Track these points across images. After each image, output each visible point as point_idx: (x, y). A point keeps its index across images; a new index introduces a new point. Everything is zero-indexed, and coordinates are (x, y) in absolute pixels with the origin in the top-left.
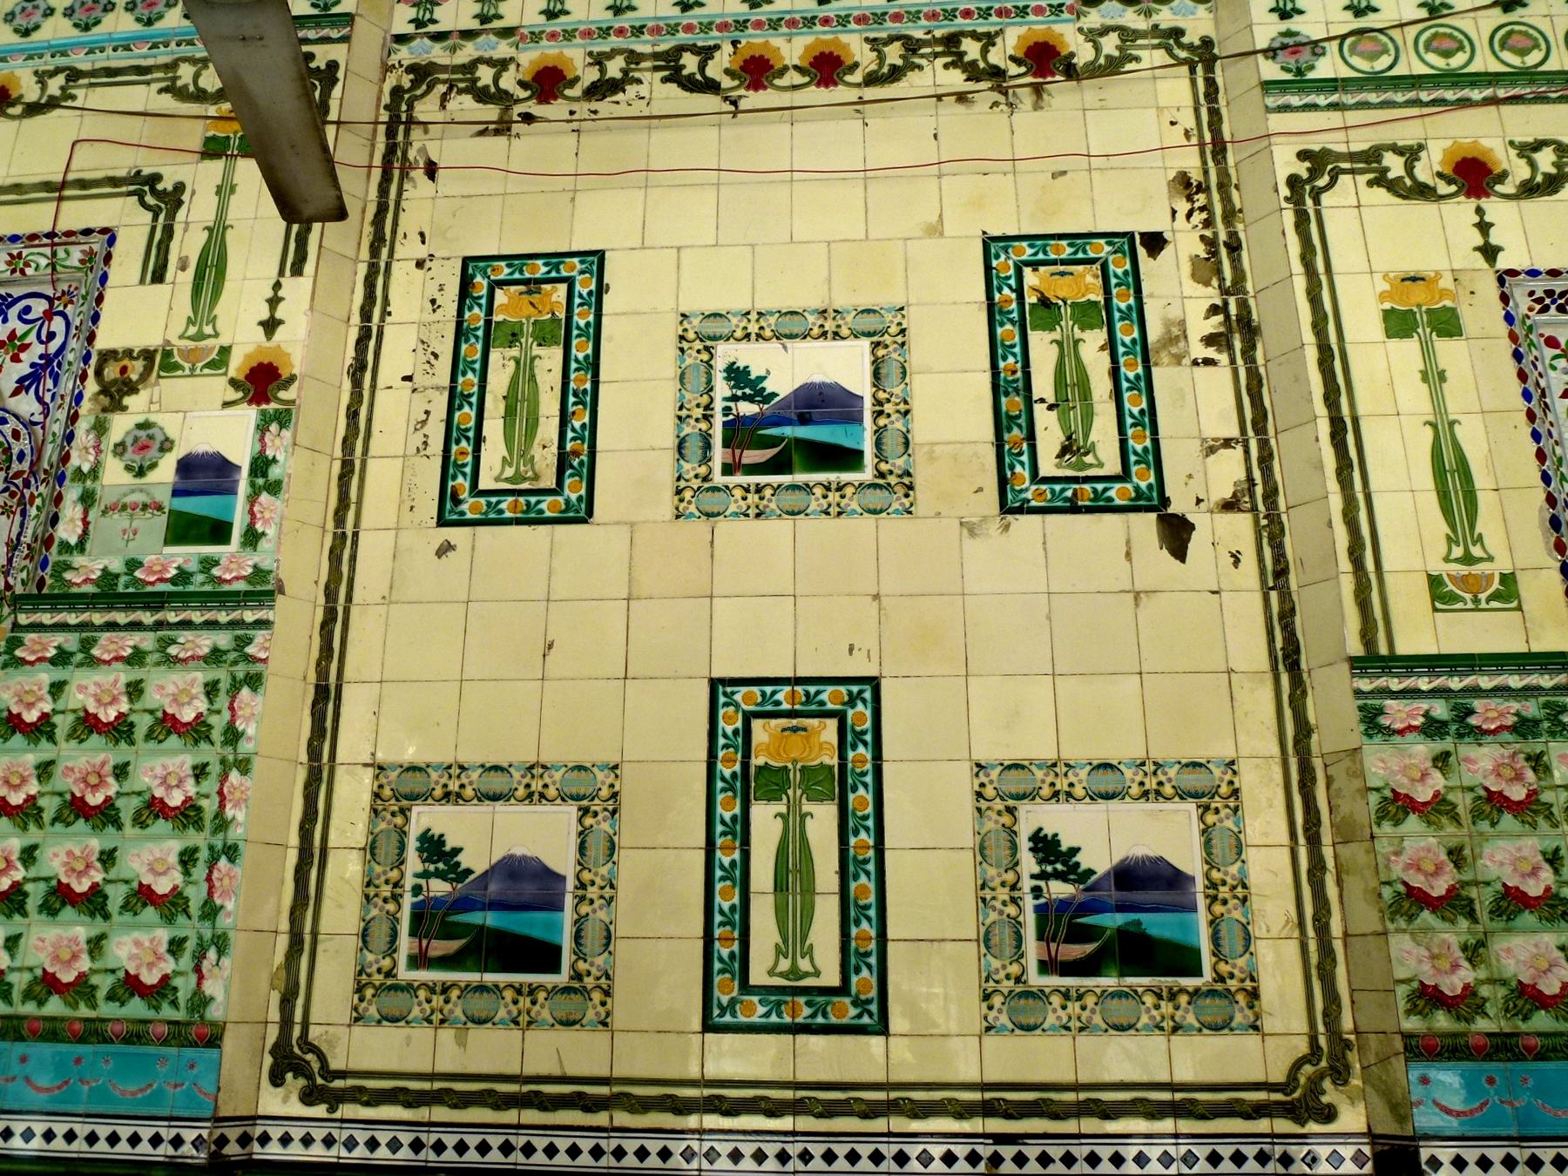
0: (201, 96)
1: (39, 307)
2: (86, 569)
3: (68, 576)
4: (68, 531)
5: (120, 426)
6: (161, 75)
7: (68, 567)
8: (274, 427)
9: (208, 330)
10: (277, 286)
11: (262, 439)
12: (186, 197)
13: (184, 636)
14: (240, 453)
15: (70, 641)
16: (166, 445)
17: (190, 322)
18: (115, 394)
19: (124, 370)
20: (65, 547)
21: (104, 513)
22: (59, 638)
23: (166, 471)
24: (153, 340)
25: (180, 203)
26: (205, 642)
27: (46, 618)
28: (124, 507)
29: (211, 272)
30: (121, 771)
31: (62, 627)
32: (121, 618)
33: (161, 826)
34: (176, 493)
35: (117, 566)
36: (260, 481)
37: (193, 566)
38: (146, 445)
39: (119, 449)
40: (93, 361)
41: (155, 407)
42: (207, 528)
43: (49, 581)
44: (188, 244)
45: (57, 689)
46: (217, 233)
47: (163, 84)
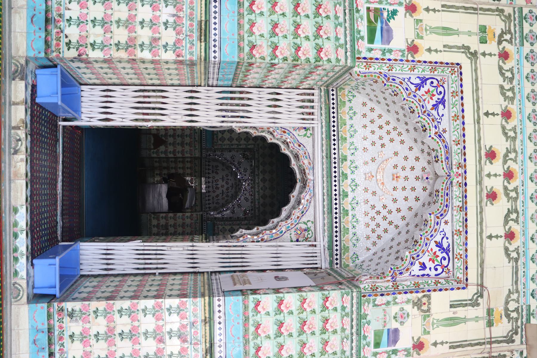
0: (507, 303)
2: (369, 309)
3: (366, 304)
4: (380, 300)
5: (408, 308)
6: (515, 288)
7: (369, 303)
8: (406, 353)
10: (447, 342)
11: (403, 350)
12: (475, 307)
13: (349, 342)
14: (399, 346)
15: (348, 310)
16: (402, 323)
17: (438, 320)
18: (418, 304)
19: (424, 304)
20: (374, 300)
21: (384, 310)
22: (349, 306)
23: (394, 325)
24: (433, 311)
25: (473, 307)
26: (347, 349)
27: (355, 301)
28: (385, 315)
29: (452, 321)
30: (313, 333)
31: (352, 307)
32: (354, 323)
33: (299, 348)
34: (388, 330)
35: (368, 318)
36: (391, 353)
37: (368, 340)
38: (402, 317)
39: (402, 309)
40: (428, 293)
41: (413, 317)
42: (378, 341)
43: (365, 298)
44: (461, 312)
45: (335, 309)
46: (465, 320)
47: (511, 290)
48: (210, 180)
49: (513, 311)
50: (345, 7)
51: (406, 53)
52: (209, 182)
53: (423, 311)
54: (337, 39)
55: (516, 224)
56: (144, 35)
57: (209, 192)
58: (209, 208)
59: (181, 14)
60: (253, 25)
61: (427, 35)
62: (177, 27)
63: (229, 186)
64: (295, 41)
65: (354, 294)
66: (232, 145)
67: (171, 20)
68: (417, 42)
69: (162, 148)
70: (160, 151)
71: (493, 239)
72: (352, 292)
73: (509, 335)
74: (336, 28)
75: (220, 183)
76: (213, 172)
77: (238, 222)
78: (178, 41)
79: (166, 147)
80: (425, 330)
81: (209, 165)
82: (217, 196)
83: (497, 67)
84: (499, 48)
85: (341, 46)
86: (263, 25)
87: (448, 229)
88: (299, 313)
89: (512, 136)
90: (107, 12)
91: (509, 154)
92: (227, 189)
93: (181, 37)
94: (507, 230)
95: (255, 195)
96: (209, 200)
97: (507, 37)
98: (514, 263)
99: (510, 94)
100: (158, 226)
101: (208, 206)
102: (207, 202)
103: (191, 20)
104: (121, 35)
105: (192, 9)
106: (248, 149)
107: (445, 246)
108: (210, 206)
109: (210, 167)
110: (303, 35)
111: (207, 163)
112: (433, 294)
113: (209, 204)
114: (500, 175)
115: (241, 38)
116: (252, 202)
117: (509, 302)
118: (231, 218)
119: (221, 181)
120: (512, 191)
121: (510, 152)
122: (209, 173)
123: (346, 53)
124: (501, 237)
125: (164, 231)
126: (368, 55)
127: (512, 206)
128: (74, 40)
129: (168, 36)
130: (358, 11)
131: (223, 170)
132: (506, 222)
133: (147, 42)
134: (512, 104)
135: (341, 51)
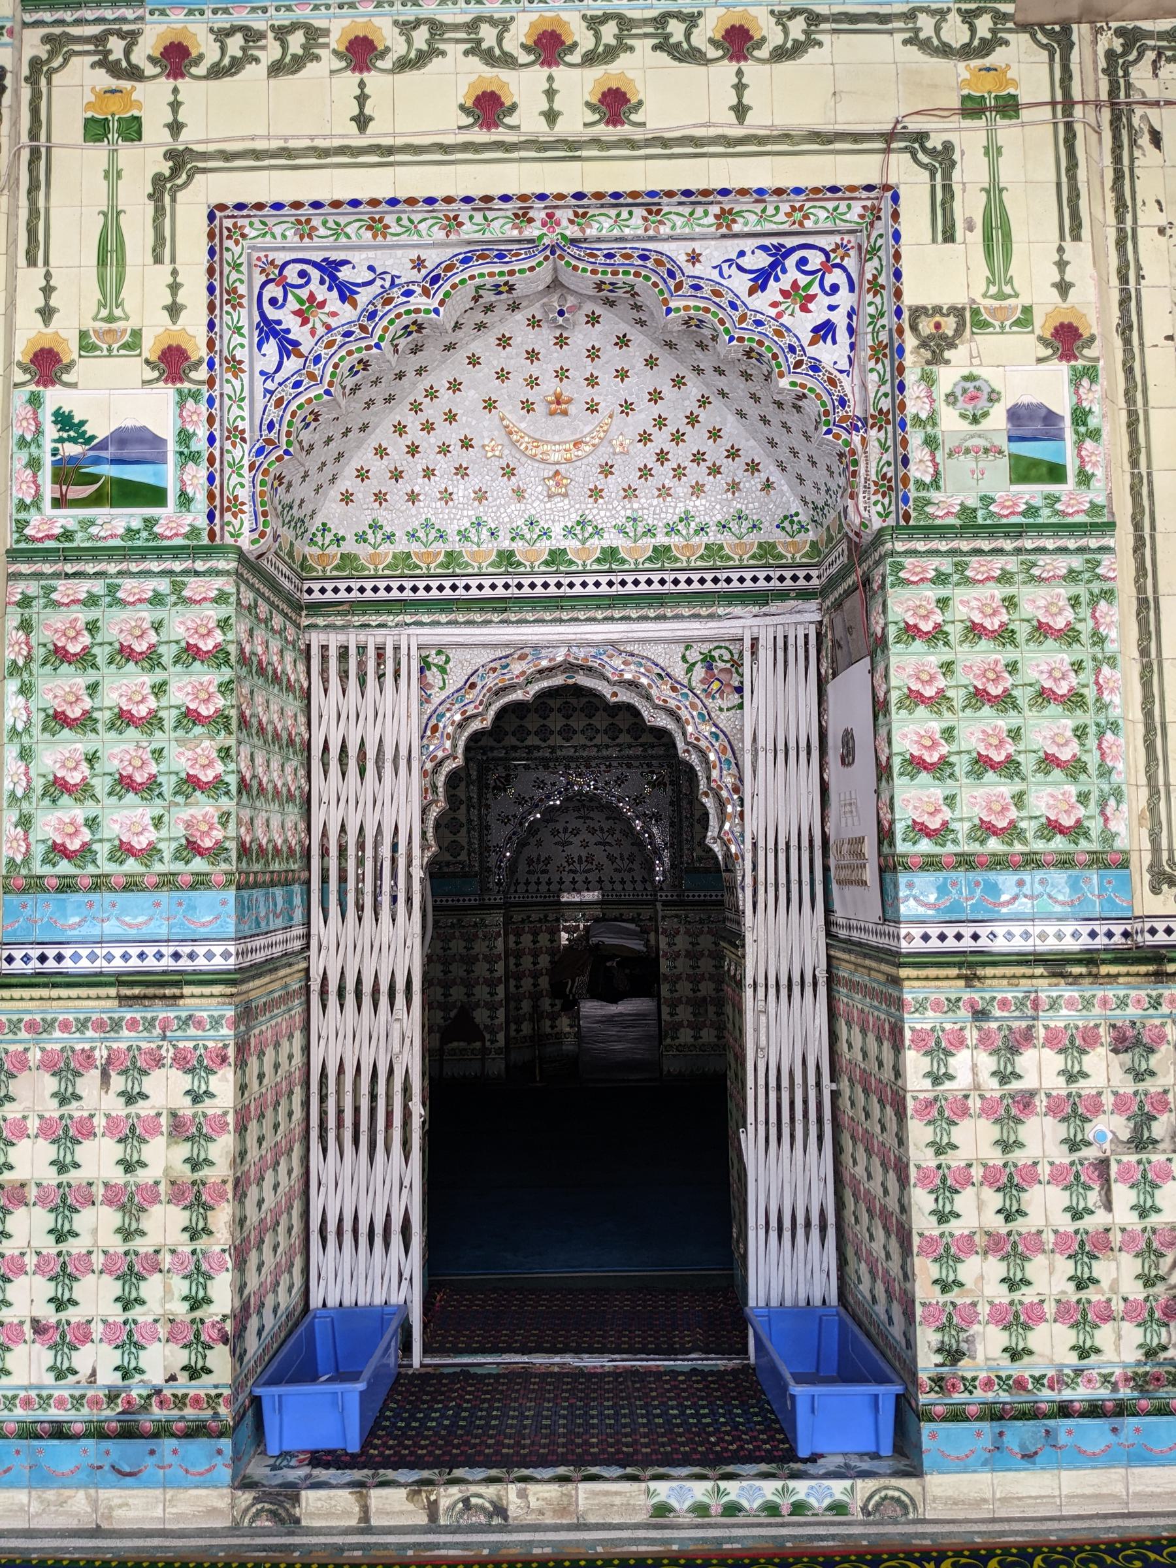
0: (945, 51)
1: (815, 260)
2: (946, 504)
3: (930, 509)
4: (920, 470)
5: (947, 378)
6: (901, 25)
7: (929, 503)
8: (1085, 382)
9: (1007, 290)
10: (1061, 250)
11: (1077, 392)
12: (956, 156)
13: (1042, 560)
14: (1062, 405)
15: (946, 565)
16: (994, 397)
17: (990, 282)
18: (937, 348)
19: (938, 326)
20: (921, 485)
21: (950, 455)
22: (935, 562)
23: (997, 420)
24: (960, 299)
25: (953, 164)
26: (1062, 564)
27: (921, 546)
28: (967, 451)
29: (997, 234)
30: (1012, 667)
31: (936, 553)
32: (986, 545)
33: (1054, 709)
34: (1011, 439)
35: (972, 502)
36: (1082, 429)
37: (1038, 502)
38: (974, 396)
39: (951, 399)
40: (906, 315)
41: (976, 361)
42: (1044, 470)
43: (913, 514)
44: (969, 205)
45: (943, 603)
46: (994, 191)
47: (907, 35)
48: (568, 878)
49: (973, 30)
50: (56, 575)
51: (186, 385)
52: (574, 882)
53: (959, 332)
54: (157, 600)
55: (701, 22)
56: (162, 1158)
57: (600, 881)
58: (644, 881)
59: (100, 1054)
60: (124, 850)
61: (127, 318)
62: (137, 1067)
63: (583, 828)
64: (169, 724)
65: (900, 546)
66: (470, 821)
67: (118, 1082)
68: (150, 347)
69: (481, 1016)
70: (488, 1022)
71: (745, 101)
72: (893, 553)
73: (1045, 41)
74: (123, 603)
75: (575, 850)
76: (545, 872)
77: (684, 803)
78: (182, 1061)
79: (477, 1005)
80: (1017, 323)
81: (527, 883)
82: (611, 858)
83: (213, 84)
84: (154, 77)
85: (177, 588)
86: (128, 819)
87: (715, 252)
88: (950, 709)
89: (427, 35)
90: (98, 1266)
91: (484, 46)
92: (592, 831)
93: (168, 1053)
94: (720, 53)
95: (610, 758)
96: (623, 882)
97: (116, 46)
98: (823, 26)
99: (296, 41)
100: (696, 1027)
101: (639, 886)
102: (629, 886)
103: (116, 1025)
104: (165, 1224)
105: (83, 1025)
106: (480, 777)
107: (763, 260)
108: (638, 878)
109: (533, 878)
110: (152, 703)
111: (521, 888)
112: (910, 299)
113: (634, 882)
114: (550, 78)
115: (168, 882)
116: (629, 766)
117: (945, 44)
118: (672, 824)
119: (569, 850)
120: (598, 36)
121: (479, 42)
122: (549, 883)
123: (197, 573)
124: (740, 73)
125: (711, 1009)
126: (201, 504)
127: (646, 35)
128: (182, 1357)
129: (166, 1089)
130: (67, 535)
131: (539, 843)
132: (693, 56)
133: (184, 1150)
134: (326, 32)
135: (194, 587)
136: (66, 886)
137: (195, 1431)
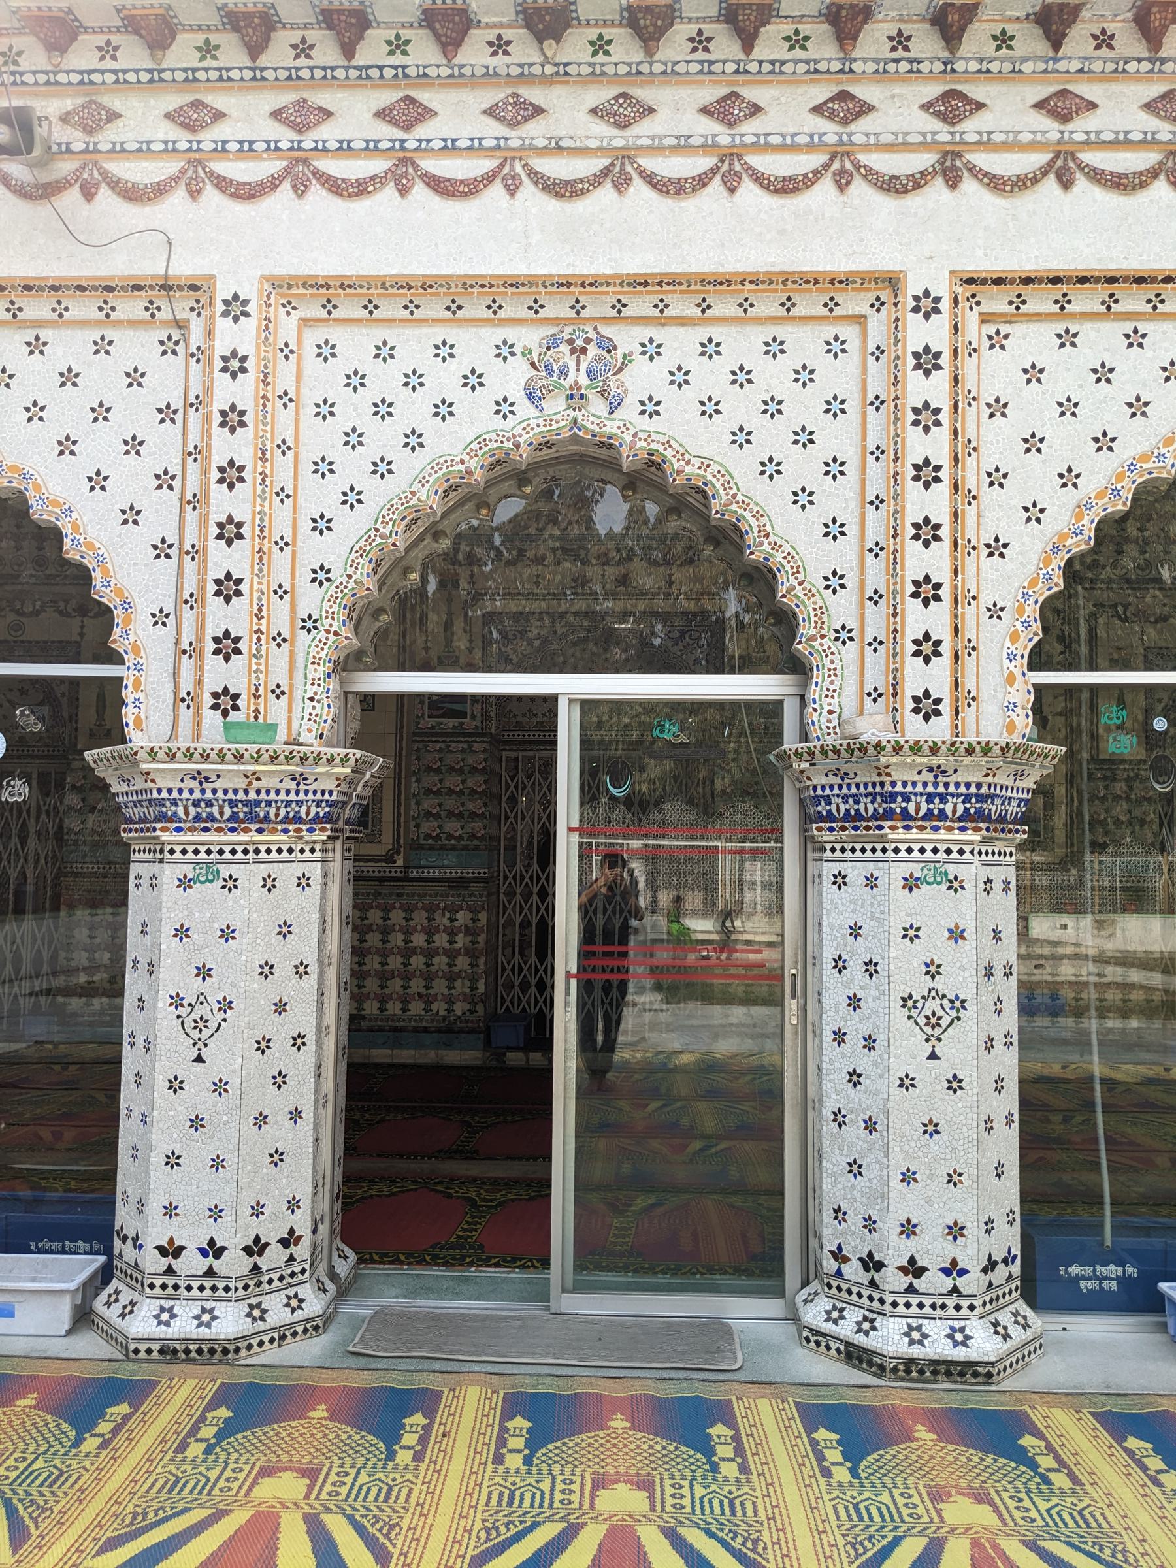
54: (463, 750)
56: (461, 940)
59: (442, 905)
60: (450, 837)
62: (454, 910)
67: (448, 915)
78: (469, 909)
86: (453, 827)
93: (464, 905)
103: (447, 896)
104: (462, 963)
105: (436, 895)
115: (466, 848)
126: (479, 718)
128: (468, 1007)
129: (462, 917)
130: (433, 727)
133: (469, 938)
135: (476, 747)
136: (431, 848)
137: (471, 1031)
